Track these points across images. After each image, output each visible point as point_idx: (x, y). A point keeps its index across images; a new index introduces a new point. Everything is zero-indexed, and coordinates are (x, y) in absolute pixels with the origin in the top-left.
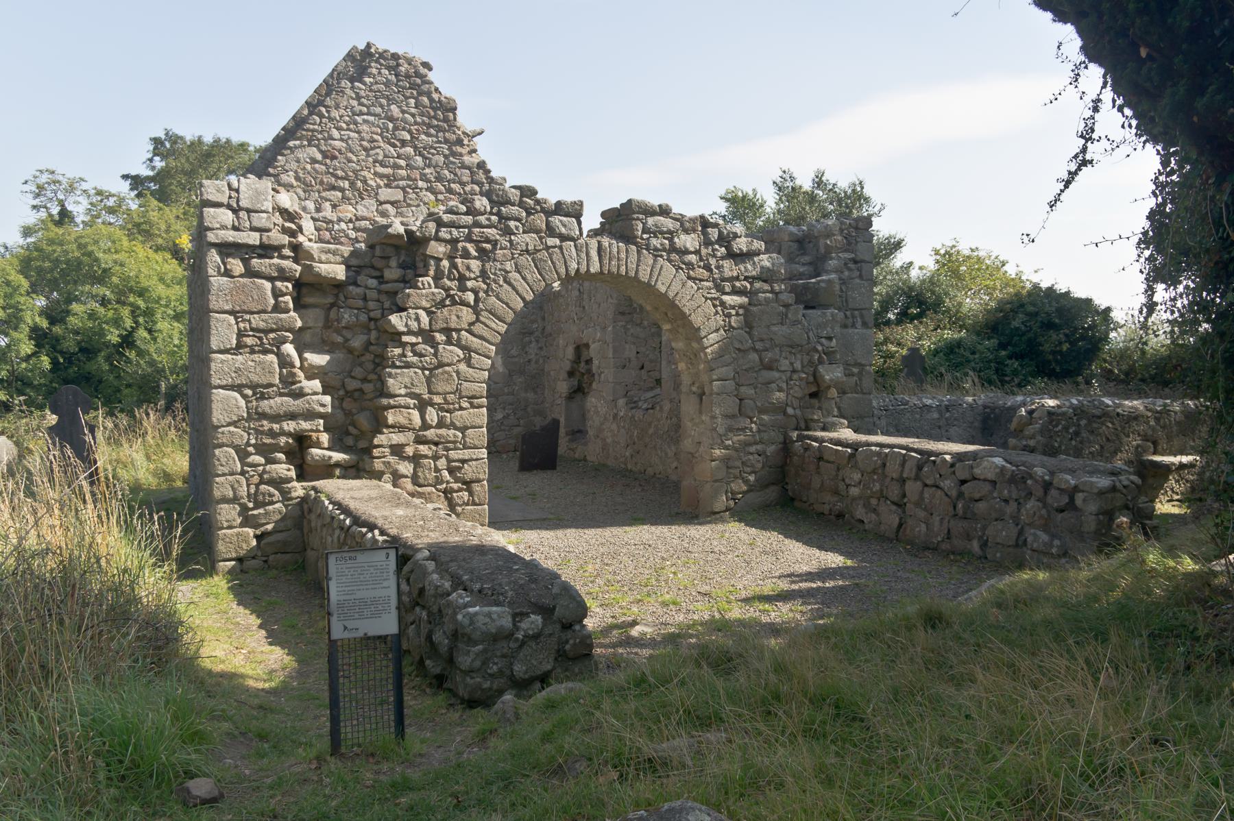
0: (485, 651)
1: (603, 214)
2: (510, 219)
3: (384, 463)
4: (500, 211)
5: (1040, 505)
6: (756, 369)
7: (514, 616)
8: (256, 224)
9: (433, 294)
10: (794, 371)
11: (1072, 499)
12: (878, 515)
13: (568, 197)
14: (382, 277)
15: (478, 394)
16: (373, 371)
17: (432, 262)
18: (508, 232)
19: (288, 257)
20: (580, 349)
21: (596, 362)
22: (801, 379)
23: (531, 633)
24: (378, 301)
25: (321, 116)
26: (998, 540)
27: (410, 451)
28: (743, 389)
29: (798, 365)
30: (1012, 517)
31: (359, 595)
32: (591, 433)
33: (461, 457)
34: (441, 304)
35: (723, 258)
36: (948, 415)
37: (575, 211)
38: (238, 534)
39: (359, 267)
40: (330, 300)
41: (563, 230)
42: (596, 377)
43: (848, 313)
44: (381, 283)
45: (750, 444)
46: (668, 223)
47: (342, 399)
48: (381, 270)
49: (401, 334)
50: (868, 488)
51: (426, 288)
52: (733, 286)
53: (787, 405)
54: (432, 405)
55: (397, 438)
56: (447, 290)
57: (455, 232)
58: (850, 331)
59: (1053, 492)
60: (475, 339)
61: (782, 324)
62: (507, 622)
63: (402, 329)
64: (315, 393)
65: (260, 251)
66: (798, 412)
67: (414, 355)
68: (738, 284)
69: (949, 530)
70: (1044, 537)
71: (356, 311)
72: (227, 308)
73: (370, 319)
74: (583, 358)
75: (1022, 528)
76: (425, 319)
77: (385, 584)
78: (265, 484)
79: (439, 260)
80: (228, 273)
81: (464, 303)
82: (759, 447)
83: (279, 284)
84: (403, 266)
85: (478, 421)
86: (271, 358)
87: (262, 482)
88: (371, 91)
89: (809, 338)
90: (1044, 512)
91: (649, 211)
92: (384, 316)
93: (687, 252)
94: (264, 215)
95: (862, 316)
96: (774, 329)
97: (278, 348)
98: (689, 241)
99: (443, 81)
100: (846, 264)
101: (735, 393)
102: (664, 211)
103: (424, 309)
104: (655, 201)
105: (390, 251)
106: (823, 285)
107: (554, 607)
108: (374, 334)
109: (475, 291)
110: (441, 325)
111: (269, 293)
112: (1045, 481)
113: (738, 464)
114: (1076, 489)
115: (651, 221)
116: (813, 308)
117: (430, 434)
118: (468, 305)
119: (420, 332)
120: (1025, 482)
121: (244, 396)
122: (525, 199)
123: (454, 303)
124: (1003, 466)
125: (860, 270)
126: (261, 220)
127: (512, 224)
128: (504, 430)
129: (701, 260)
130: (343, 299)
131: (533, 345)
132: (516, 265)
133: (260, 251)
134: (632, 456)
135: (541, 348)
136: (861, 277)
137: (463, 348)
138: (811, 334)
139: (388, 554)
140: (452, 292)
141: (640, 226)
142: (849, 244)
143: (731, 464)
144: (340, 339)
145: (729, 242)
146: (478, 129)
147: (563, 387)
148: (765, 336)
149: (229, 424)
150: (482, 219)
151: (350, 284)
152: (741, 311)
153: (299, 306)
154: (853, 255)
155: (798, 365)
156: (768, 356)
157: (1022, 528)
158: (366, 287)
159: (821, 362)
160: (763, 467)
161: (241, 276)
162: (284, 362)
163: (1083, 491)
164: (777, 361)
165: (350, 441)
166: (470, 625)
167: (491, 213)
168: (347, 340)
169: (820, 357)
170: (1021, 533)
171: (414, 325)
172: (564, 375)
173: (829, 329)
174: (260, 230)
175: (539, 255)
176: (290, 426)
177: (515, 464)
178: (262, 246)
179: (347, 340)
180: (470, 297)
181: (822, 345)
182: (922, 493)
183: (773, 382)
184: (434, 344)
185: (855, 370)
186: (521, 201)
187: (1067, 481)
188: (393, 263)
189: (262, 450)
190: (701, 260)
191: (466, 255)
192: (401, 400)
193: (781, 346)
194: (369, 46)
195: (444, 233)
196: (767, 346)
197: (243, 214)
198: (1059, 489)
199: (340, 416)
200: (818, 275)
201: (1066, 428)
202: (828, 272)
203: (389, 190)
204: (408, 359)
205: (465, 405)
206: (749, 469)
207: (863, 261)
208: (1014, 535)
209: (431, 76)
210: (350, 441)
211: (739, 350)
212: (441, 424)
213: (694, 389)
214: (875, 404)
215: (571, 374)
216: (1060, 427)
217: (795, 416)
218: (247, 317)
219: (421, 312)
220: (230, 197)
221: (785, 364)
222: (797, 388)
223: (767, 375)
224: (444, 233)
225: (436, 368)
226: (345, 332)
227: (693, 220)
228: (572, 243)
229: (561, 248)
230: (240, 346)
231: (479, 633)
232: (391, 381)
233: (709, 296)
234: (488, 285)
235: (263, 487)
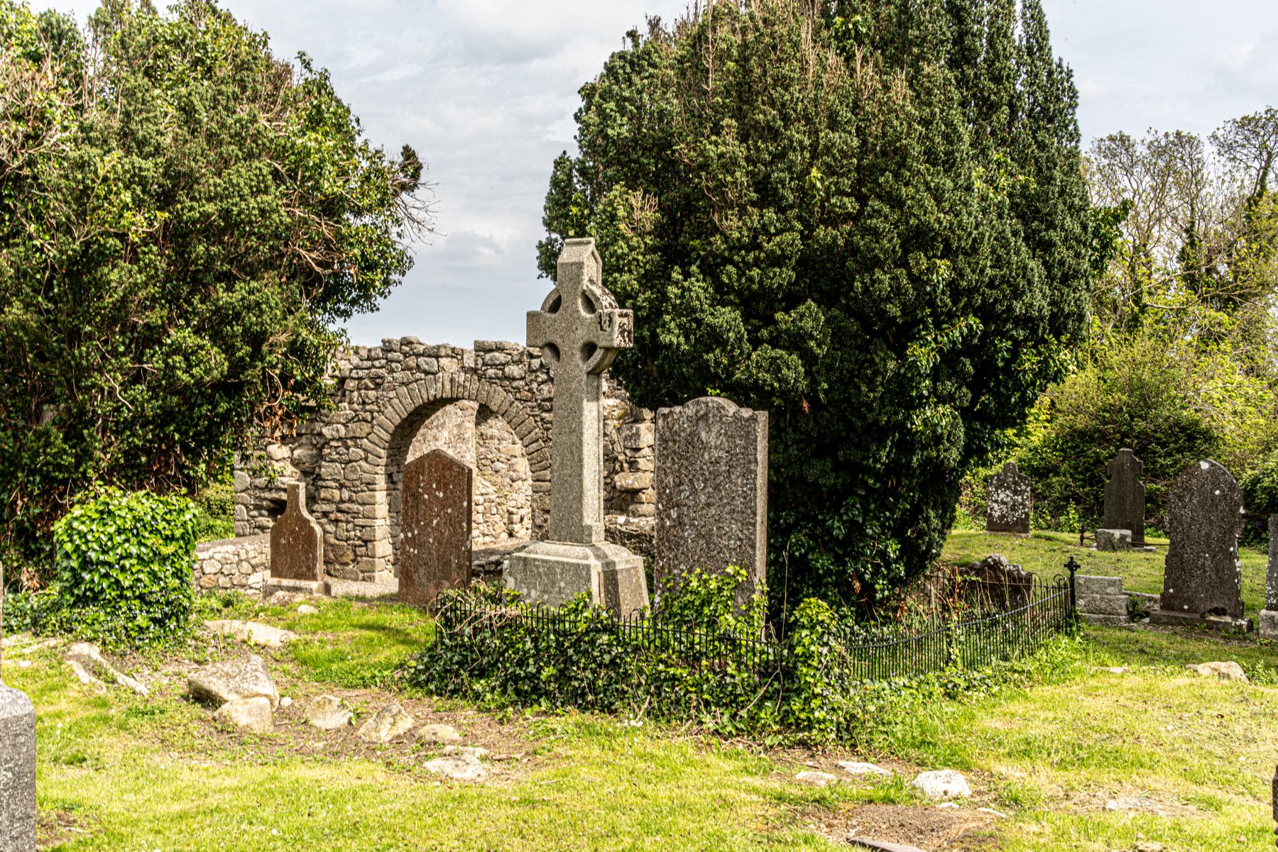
18: (392, 371)
27: (332, 516)
35: (543, 383)
46: (501, 357)
55: (326, 508)
56: (355, 411)
81: (365, 420)
98: (515, 370)
102: (500, 348)
109: (372, 412)
110: (351, 434)
115: (488, 356)
117: (344, 506)
118: (367, 421)
119: (340, 439)
127: (394, 365)
137: (364, 450)
150: (377, 363)
184: (348, 448)
191: (367, 388)
212: (351, 500)
219: (340, 426)
224: (354, 374)
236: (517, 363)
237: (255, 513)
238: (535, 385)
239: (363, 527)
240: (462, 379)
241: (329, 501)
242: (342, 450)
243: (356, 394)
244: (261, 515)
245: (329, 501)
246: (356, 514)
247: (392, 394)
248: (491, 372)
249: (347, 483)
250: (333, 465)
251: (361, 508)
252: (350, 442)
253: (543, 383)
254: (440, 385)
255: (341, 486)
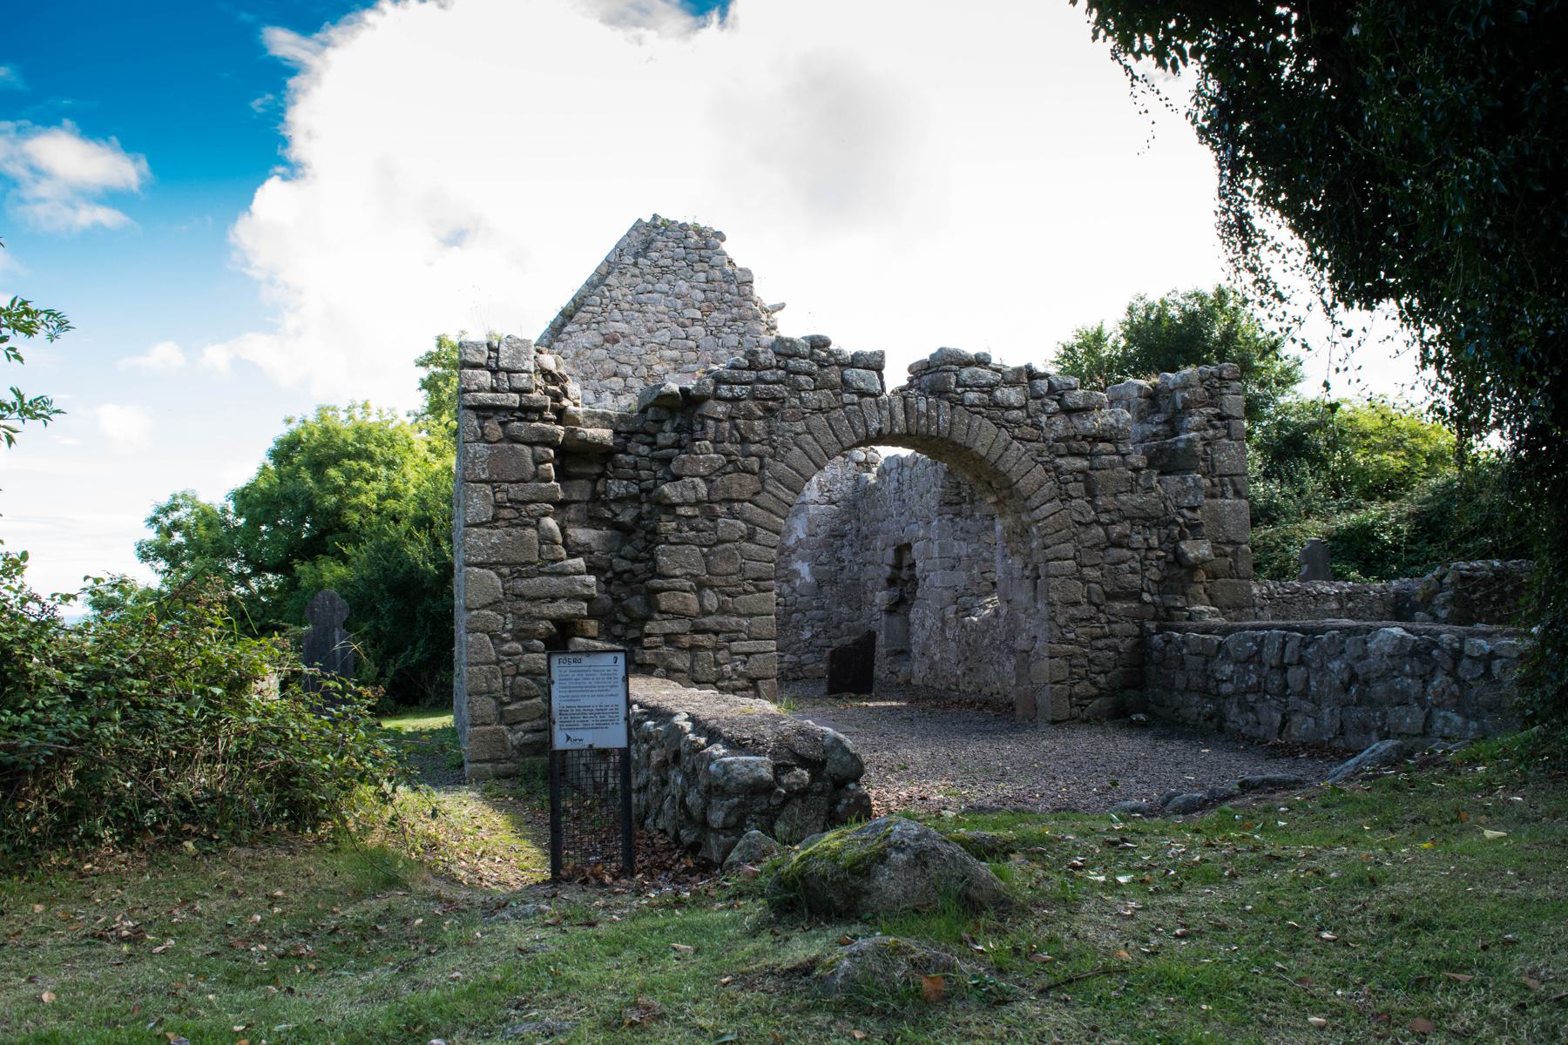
0: (741, 805)
1: (910, 369)
2: (798, 373)
3: (656, 654)
4: (787, 364)
5: (1450, 680)
6: (1102, 546)
7: (776, 768)
8: (517, 384)
9: (712, 459)
10: (1150, 549)
11: (1488, 669)
12: (1256, 714)
13: (868, 347)
14: (655, 443)
15: (764, 576)
16: (645, 549)
17: (711, 423)
18: (797, 389)
19: (551, 420)
20: (902, 549)
21: (919, 564)
22: (1159, 558)
23: (796, 788)
24: (650, 469)
25: (602, 296)
26: (1403, 729)
27: (686, 641)
28: (1086, 571)
29: (1154, 541)
30: (1417, 699)
31: (585, 702)
32: (915, 650)
33: (745, 649)
34: (722, 471)
35: (1054, 414)
36: (1350, 605)
37: (874, 363)
38: (494, 733)
39: (627, 432)
40: (597, 470)
41: (862, 385)
42: (920, 582)
43: (1216, 480)
44: (653, 450)
45: (1098, 638)
46: (987, 375)
47: (608, 582)
48: (653, 435)
49: (674, 506)
50: (1243, 681)
51: (706, 454)
52: (1069, 448)
53: (1142, 590)
54: (711, 587)
55: (671, 626)
57: (737, 389)
58: (1220, 501)
59: (1466, 662)
60: (759, 510)
61: (1132, 491)
62: (766, 773)
63: (676, 499)
64: (580, 573)
65: (518, 414)
66: (1156, 598)
67: (691, 530)
68: (1074, 445)
69: (1342, 726)
70: (1458, 720)
71: (625, 482)
72: (483, 477)
73: (642, 491)
74: (906, 562)
75: (1430, 712)
76: (703, 489)
77: (613, 691)
78: (521, 674)
79: (718, 420)
80: (483, 438)
82: (1108, 641)
83: (539, 449)
84: (677, 430)
85: (766, 608)
86: (530, 532)
87: (518, 674)
88: (657, 266)
89: (1166, 507)
90: (1455, 688)
91: (967, 362)
92: (656, 486)
93: (1010, 407)
94: (526, 375)
95: (1233, 484)
96: (1123, 498)
97: (538, 522)
98: (1012, 395)
99: (737, 251)
100: (1209, 421)
101: (1077, 575)
102: (982, 361)
103: (702, 477)
104: (971, 349)
105: (663, 414)
106: (1181, 445)
107: (824, 761)
108: (646, 507)
110: (721, 495)
111: (529, 460)
112: (1453, 649)
113: (1084, 661)
114: (1492, 655)
115: (966, 373)
116: (1170, 473)
118: (752, 473)
119: (698, 503)
120: (1430, 654)
121: (501, 575)
122: (817, 351)
123: (737, 470)
124: (1403, 637)
125: (1227, 427)
126: (521, 381)
127: (802, 379)
128: (813, 652)
129: (1029, 416)
130: (611, 469)
131: (844, 551)
132: (807, 425)
133: (518, 414)
134: (964, 674)
135: (856, 554)
136: (1229, 436)
137: (746, 521)
138: (1168, 503)
139: (616, 658)
140: (733, 457)
141: (953, 379)
142: (1212, 397)
143: (1075, 662)
144: (608, 514)
145: (1061, 395)
146: (777, 302)
147: (882, 597)
148: (1111, 507)
149: (484, 607)
150: (768, 375)
151: (620, 452)
152: (1080, 477)
153: (562, 476)
154: (1218, 411)
155: (1154, 541)
156: (1117, 529)
157: (1430, 712)
158: (638, 455)
159: (1183, 537)
160: (1116, 666)
161: (499, 441)
162: (546, 539)
163: (1501, 657)
164: (1127, 536)
165: (618, 630)
166: (724, 774)
167: (779, 368)
168: (616, 515)
169: (1181, 532)
170: (1429, 718)
171: (690, 496)
172: (882, 581)
173: (1190, 497)
174: (520, 391)
175: (835, 414)
176: (551, 610)
177: (824, 688)
178: (522, 408)
179: (616, 515)
180: (754, 463)
181: (1183, 516)
182: (1307, 680)
183: (1124, 562)
185: (1228, 549)
186: (812, 353)
187: (1481, 647)
188: (667, 426)
189: (520, 636)
190: (1029, 416)
192: (677, 583)
193: (1132, 519)
194: (655, 217)
195: (724, 390)
196: (1115, 518)
197: (503, 376)
198: (1470, 657)
199: (607, 601)
200: (1177, 434)
201: (1487, 597)
202: (1188, 431)
203: (677, 376)
204: (684, 535)
205: (751, 588)
206: (1097, 669)
207: (1230, 417)
208: (1421, 722)
209: (725, 246)
210: (618, 630)
211: (1080, 523)
212: (722, 610)
213: (1027, 573)
214: (1255, 591)
215: (891, 582)
216: (1478, 595)
217: (1153, 603)
218: (505, 486)
219: (697, 480)
220: (489, 358)
221: (1137, 539)
222: (1154, 570)
223: (1116, 553)
224: (724, 390)
225: (715, 544)
226: (613, 507)
227: (1018, 371)
228: (872, 399)
229: (859, 404)
230: (495, 519)
231: (733, 784)
232: (663, 559)
233: (1039, 459)
234: (775, 448)
235: (520, 679)
236: (1012, 384)
237: (517, 646)
238: (1044, 418)
239: (748, 654)
240: (923, 406)
241: (678, 615)
242: (703, 523)
243: (727, 425)
244: (527, 650)
245: (678, 615)
246: (733, 635)
247: (799, 427)
248: (972, 396)
249: (716, 581)
250: (686, 549)
251: (745, 622)
252: (719, 509)
253: (1054, 414)
254: (885, 413)
255: (701, 586)
